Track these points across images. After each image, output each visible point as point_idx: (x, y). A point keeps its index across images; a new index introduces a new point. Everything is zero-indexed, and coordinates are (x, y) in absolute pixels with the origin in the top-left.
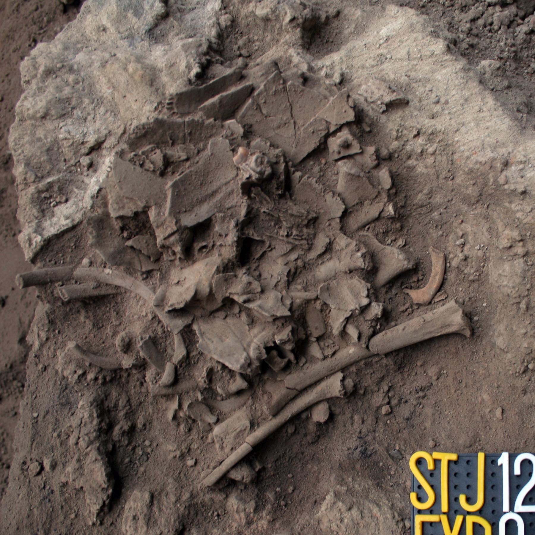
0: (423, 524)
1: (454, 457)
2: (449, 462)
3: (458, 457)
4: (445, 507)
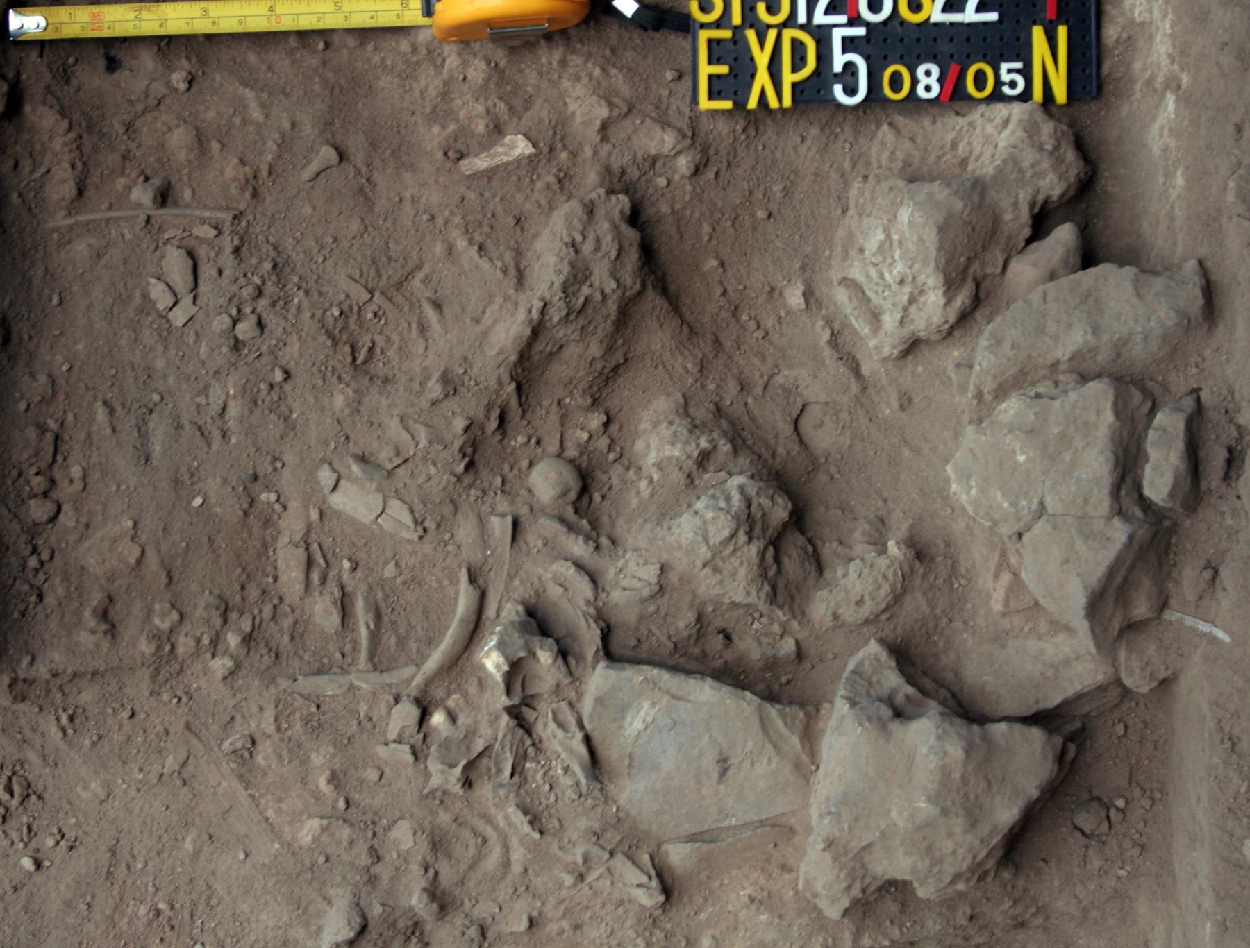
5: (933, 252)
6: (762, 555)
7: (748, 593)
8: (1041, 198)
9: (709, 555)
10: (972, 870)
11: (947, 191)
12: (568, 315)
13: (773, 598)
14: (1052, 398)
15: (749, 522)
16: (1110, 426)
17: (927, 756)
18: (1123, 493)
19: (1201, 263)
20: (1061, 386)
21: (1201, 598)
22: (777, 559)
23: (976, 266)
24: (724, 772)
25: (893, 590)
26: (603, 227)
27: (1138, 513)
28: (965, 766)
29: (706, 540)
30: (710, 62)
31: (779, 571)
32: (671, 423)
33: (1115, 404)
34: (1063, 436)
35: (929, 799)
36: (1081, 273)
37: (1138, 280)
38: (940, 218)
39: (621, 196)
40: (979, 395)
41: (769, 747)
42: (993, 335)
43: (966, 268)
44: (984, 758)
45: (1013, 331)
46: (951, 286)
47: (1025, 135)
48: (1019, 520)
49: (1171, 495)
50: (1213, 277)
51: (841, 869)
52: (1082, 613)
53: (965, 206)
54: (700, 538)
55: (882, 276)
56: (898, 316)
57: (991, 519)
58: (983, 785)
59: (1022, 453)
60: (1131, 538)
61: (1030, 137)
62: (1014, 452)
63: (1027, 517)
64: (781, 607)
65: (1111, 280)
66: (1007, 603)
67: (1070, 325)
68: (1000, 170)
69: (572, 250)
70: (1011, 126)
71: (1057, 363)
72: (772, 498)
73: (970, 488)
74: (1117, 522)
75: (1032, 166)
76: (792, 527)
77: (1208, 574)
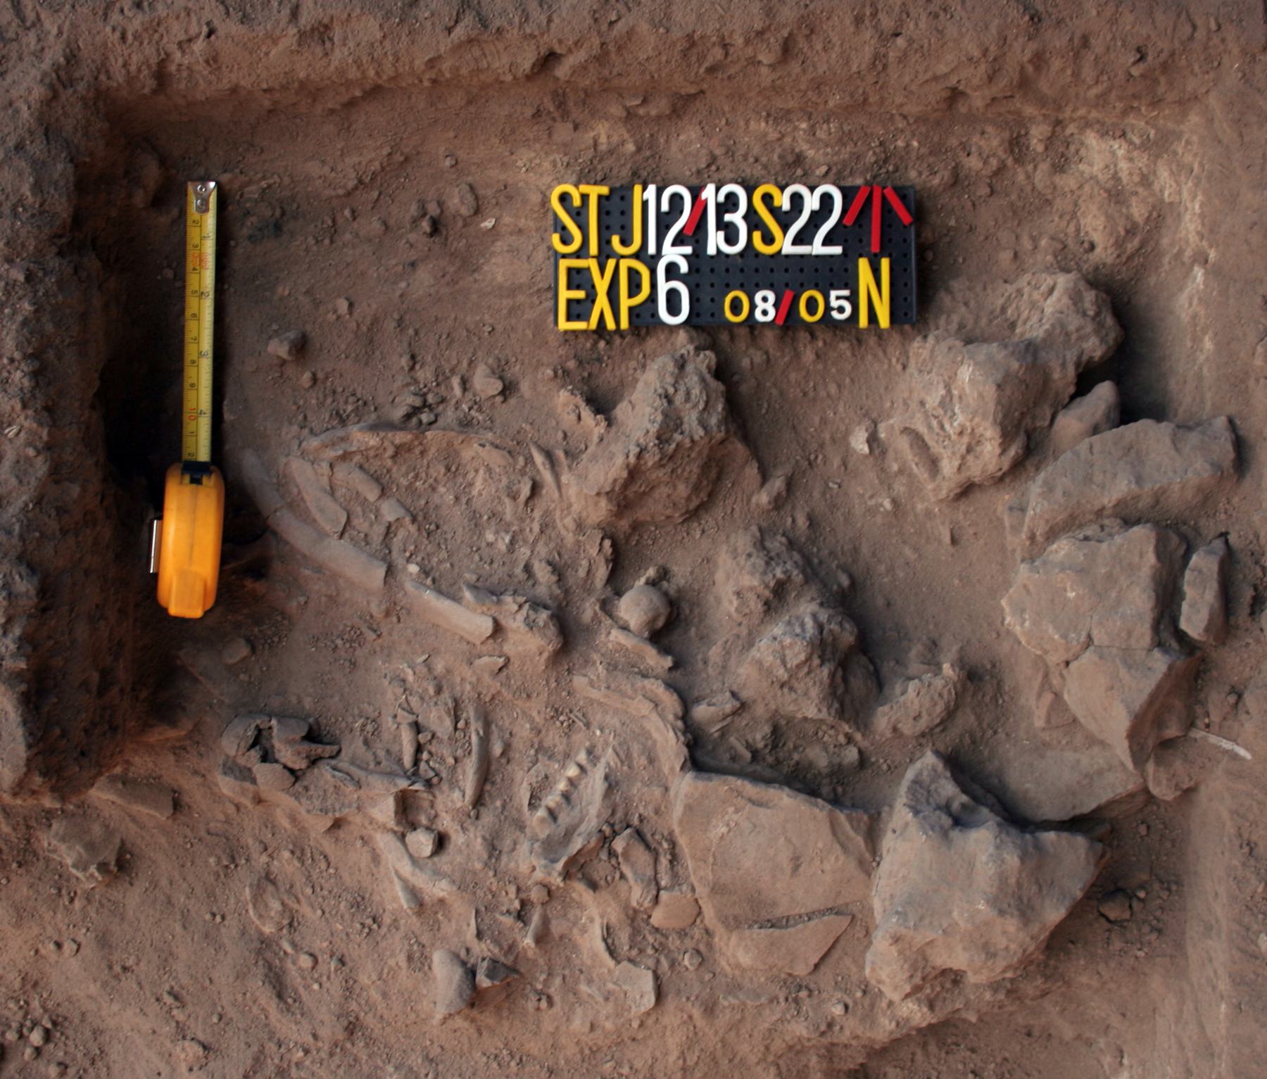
0: (570, 270)
1: (604, 190)
2: (600, 197)
3: (611, 190)
4: (593, 248)
5: (991, 406)
6: (832, 676)
7: (820, 710)
8: (1085, 358)
9: (786, 676)
10: (1020, 962)
11: (1004, 353)
12: (661, 459)
13: (841, 714)
14: (1100, 541)
15: (822, 647)
16: (1152, 567)
17: (987, 863)
18: (1162, 627)
19: (1231, 421)
20: (1107, 530)
21: (1225, 719)
22: (845, 680)
23: (1028, 420)
24: (796, 868)
25: (947, 708)
26: (692, 381)
27: (1175, 645)
28: (1020, 872)
29: (784, 663)
30: (569, 287)
31: (847, 690)
32: (749, 555)
33: (1156, 547)
34: (1109, 576)
35: (988, 902)
36: (1122, 427)
37: (1175, 435)
38: (999, 376)
39: (707, 352)
40: (1032, 538)
41: (837, 847)
42: (1046, 483)
43: (1020, 421)
44: (1036, 860)
45: (1064, 479)
46: (1007, 438)
47: (1070, 302)
48: (1068, 650)
49: (1207, 630)
50: (1241, 433)
51: (906, 961)
52: (1124, 734)
53: (1021, 367)
54: (778, 661)
55: (942, 427)
56: (956, 463)
57: (1042, 649)
58: (1034, 888)
59: (1073, 590)
60: (1170, 668)
61: (1075, 304)
62: (1065, 590)
63: (1075, 647)
64: (848, 722)
65: (1149, 434)
66: (1048, 721)
67: (1115, 475)
68: (1049, 334)
69: (664, 401)
70: (1056, 294)
71: (1103, 508)
72: (841, 624)
73: (1024, 621)
74: (1157, 654)
75: (1077, 330)
76: (860, 653)
77: (1232, 699)
